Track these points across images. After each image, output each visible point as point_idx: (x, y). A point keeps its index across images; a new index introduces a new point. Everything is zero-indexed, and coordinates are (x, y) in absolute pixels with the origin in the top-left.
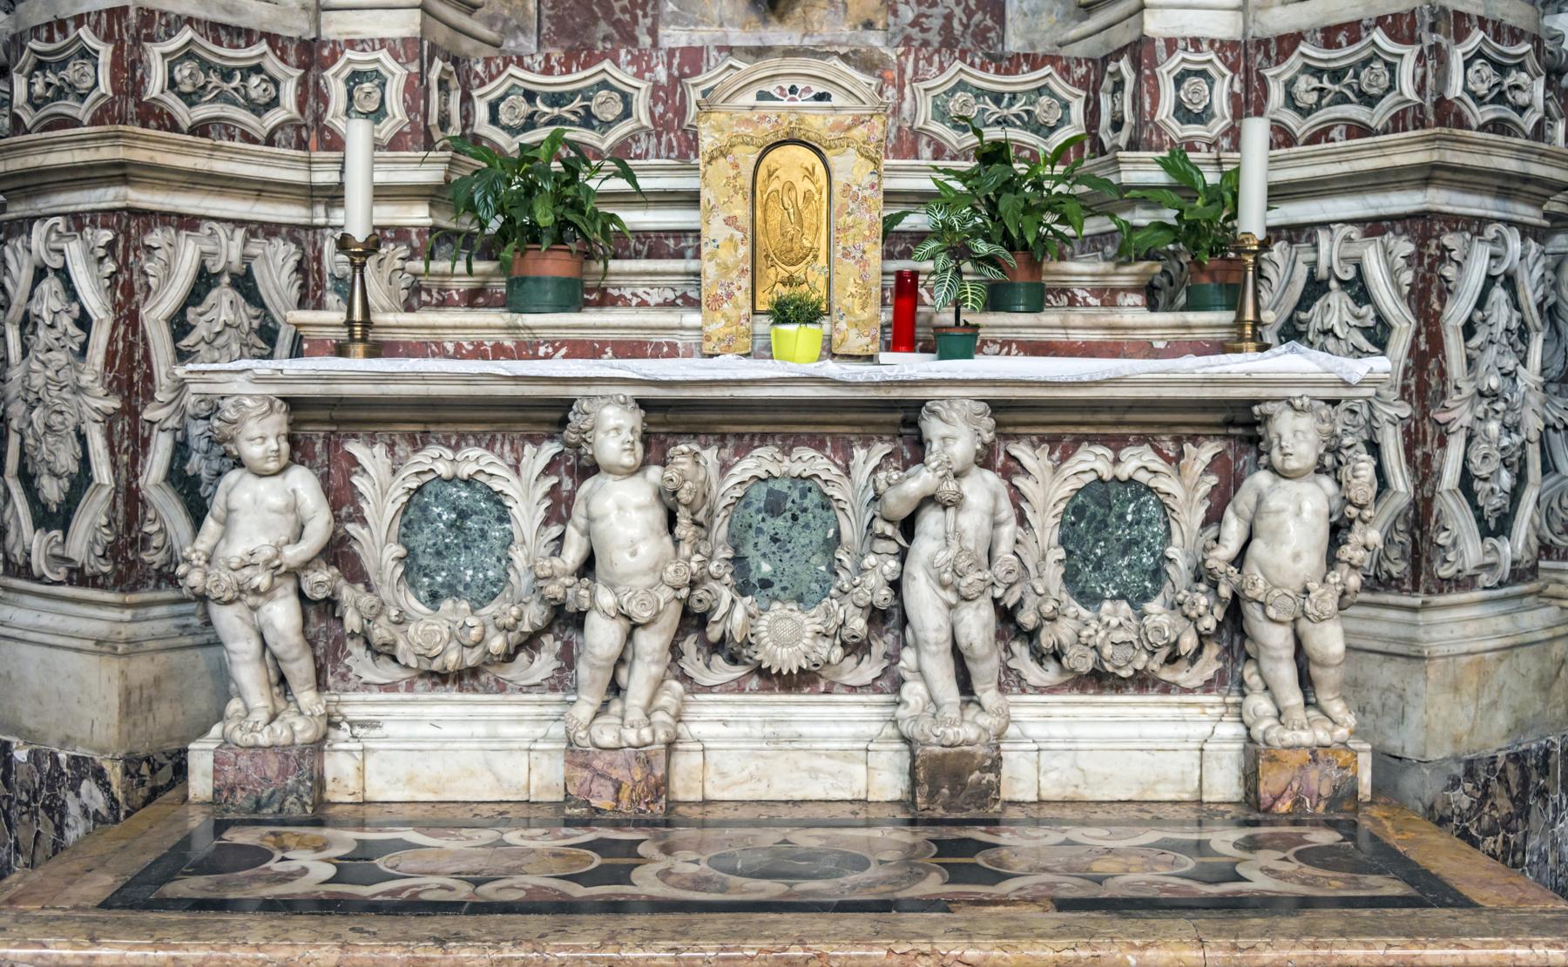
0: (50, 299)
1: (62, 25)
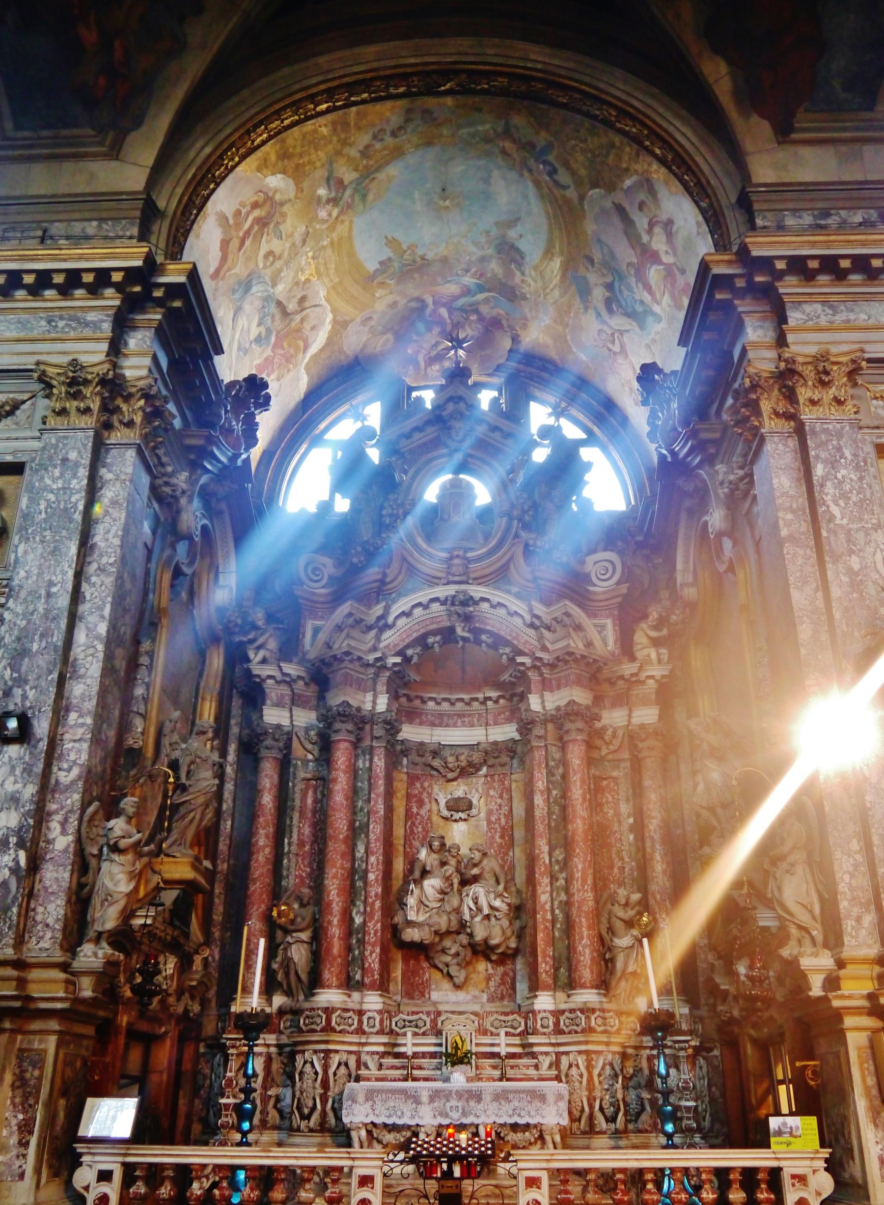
0: (308, 1068)
1: (314, 1009)
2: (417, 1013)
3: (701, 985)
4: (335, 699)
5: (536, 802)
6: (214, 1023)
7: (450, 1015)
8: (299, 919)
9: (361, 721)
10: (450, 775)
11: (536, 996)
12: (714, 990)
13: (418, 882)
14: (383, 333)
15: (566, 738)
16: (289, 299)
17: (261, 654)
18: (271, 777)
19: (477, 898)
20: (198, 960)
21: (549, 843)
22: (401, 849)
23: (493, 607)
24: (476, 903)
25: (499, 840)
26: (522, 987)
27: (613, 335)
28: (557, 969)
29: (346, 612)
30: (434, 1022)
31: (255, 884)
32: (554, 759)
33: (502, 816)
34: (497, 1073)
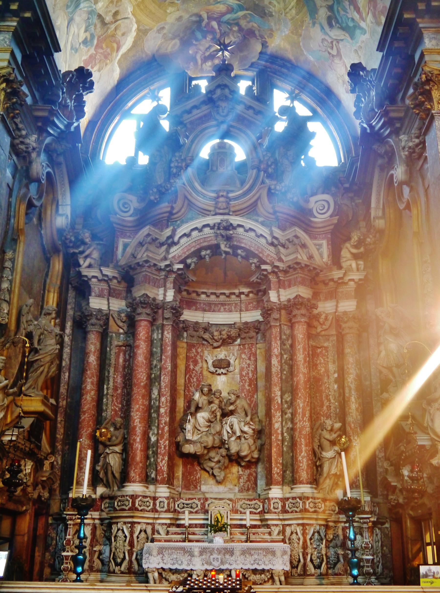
1: (124, 496)
2: (192, 499)
3: (378, 482)
4: (138, 292)
5: (273, 362)
6: (58, 504)
7: (214, 501)
8: (114, 438)
9: (155, 308)
10: (215, 344)
11: (270, 489)
12: (388, 487)
13: (193, 415)
14: (172, 39)
15: (293, 320)
16: (107, 13)
17: (88, 261)
18: (95, 344)
19: (232, 425)
20: (47, 463)
21: (281, 390)
22: (182, 392)
23: (246, 231)
24: (232, 429)
25: (247, 388)
26: (261, 483)
27: (332, 42)
28: (284, 472)
29: (146, 233)
30: (203, 505)
31: (85, 414)
32: (285, 334)
33: (250, 372)
34: (244, 537)
